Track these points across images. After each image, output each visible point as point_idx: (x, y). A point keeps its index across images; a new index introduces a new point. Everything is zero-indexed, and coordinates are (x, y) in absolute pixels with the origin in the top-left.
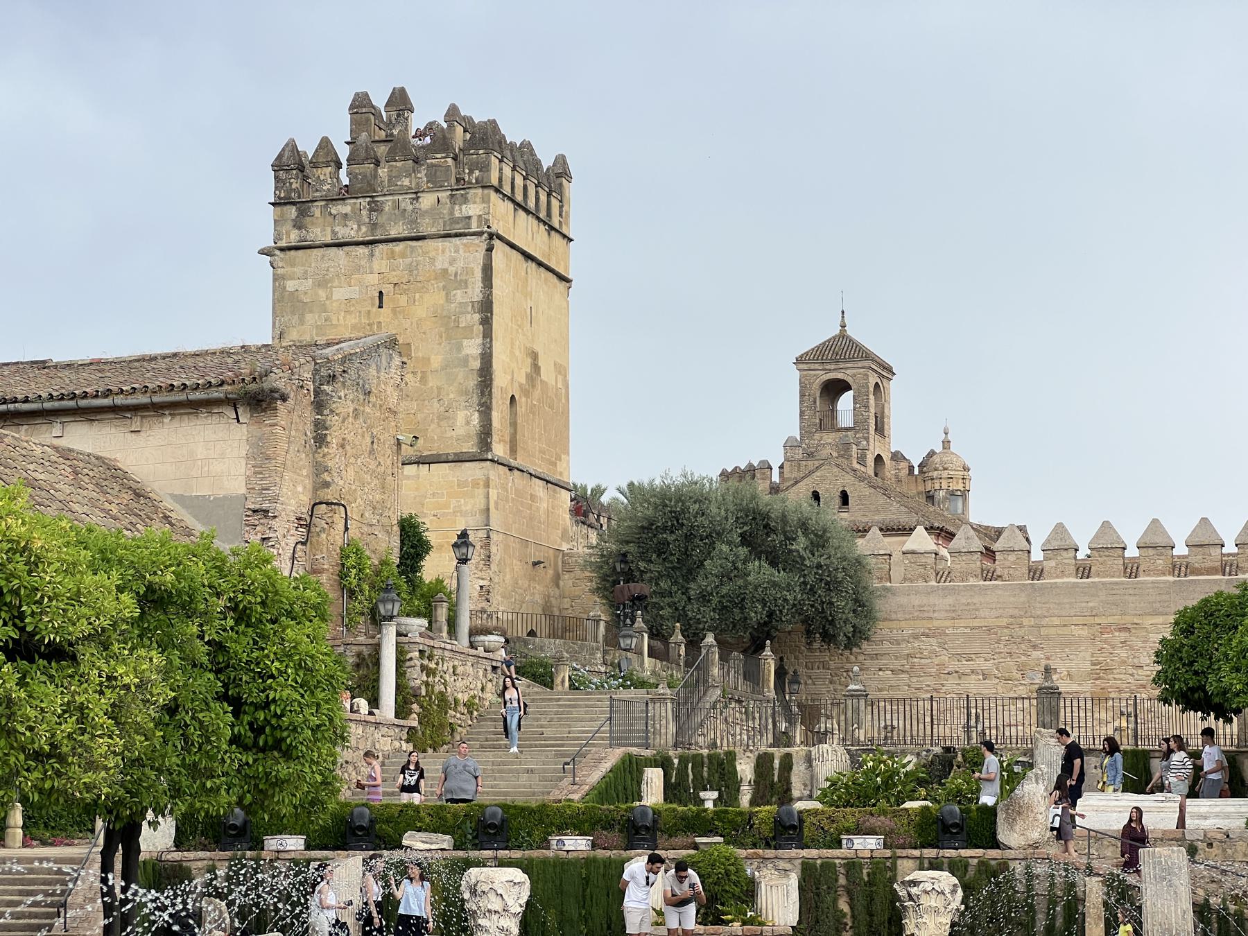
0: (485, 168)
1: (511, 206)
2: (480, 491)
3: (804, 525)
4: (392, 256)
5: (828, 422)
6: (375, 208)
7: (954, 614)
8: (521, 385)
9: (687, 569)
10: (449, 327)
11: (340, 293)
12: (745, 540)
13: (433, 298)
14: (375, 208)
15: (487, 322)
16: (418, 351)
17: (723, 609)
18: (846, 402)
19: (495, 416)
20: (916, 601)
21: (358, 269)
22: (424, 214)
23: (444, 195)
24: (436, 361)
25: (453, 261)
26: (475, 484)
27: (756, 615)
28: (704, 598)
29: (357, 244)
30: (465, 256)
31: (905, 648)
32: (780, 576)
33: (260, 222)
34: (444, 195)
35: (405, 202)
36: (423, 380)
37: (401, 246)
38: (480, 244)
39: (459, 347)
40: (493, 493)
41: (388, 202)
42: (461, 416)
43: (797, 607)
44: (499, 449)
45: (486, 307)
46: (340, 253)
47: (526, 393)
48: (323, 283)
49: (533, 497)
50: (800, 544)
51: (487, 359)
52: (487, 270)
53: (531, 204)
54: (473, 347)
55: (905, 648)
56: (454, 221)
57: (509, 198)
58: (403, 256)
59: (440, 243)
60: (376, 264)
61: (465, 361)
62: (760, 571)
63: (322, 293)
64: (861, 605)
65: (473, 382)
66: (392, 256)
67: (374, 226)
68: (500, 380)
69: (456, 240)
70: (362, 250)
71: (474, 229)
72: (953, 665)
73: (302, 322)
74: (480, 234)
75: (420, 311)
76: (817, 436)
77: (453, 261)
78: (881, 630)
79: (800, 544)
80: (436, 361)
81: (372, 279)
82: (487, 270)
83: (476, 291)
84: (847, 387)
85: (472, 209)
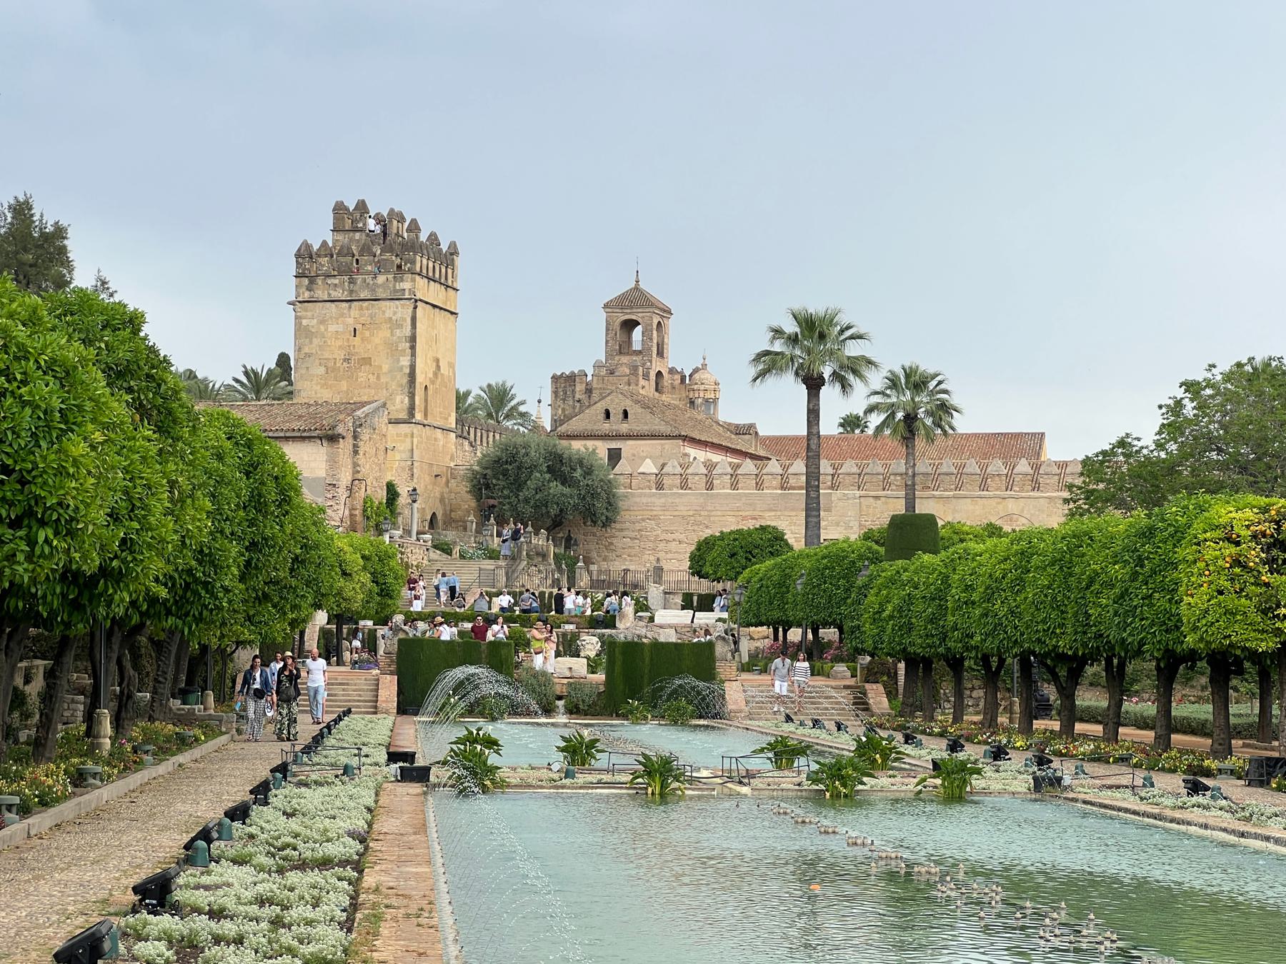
0: (413, 262)
2: (408, 440)
3: (581, 462)
4: (361, 309)
5: (624, 348)
6: (352, 281)
7: (664, 508)
9: (518, 485)
10: (393, 349)
11: (332, 328)
12: (550, 470)
13: (384, 333)
15: (413, 348)
16: (375, 362)
17: (536, 507)
18: (637, 333)
19: (417, 398)
20: (644, 500)
21: (342, 315)
22: (378, 286)
23: (390, 277)
24: (385, 368)
26: (406, 436)
27: (554, 510)
28: (527, 501)
30: (401, 311)
31: (638, 526)
32: (567, 490)
33: (288, 287)
34: (390, 277)
35: (369, 279)
36: (378, 378)
39: (398, 361)
40: (415, 440)
41: (359, 278)
42: (398, 398)
43: (575, 507)
44: (419, 416)
45: (413, 339)
46: (333, 305)
47: (433, 382)
48: (322, 322)
49: (436, 439)
50: (578, 474)
51: (413, 368)
52: (414, 319)
54: (405, 361)
55: (638, 526)
60: (352, 313)
61: (401, 369)
62: (556, 488)
63: (322, 328)
64: (611, 505)
65: (405, 380)
66: (361, 309)
67: (351, 292)
70: (344, 304)
72: (664, 536)
73: (311, 342)
75: (377, 340)
76: (617, 358)
78: (624, 516)
79: (578, 474)
80: (385, 368)
82: (414, 319)
83: (407, 331)
84: (637, 323)
85: (406, 285)
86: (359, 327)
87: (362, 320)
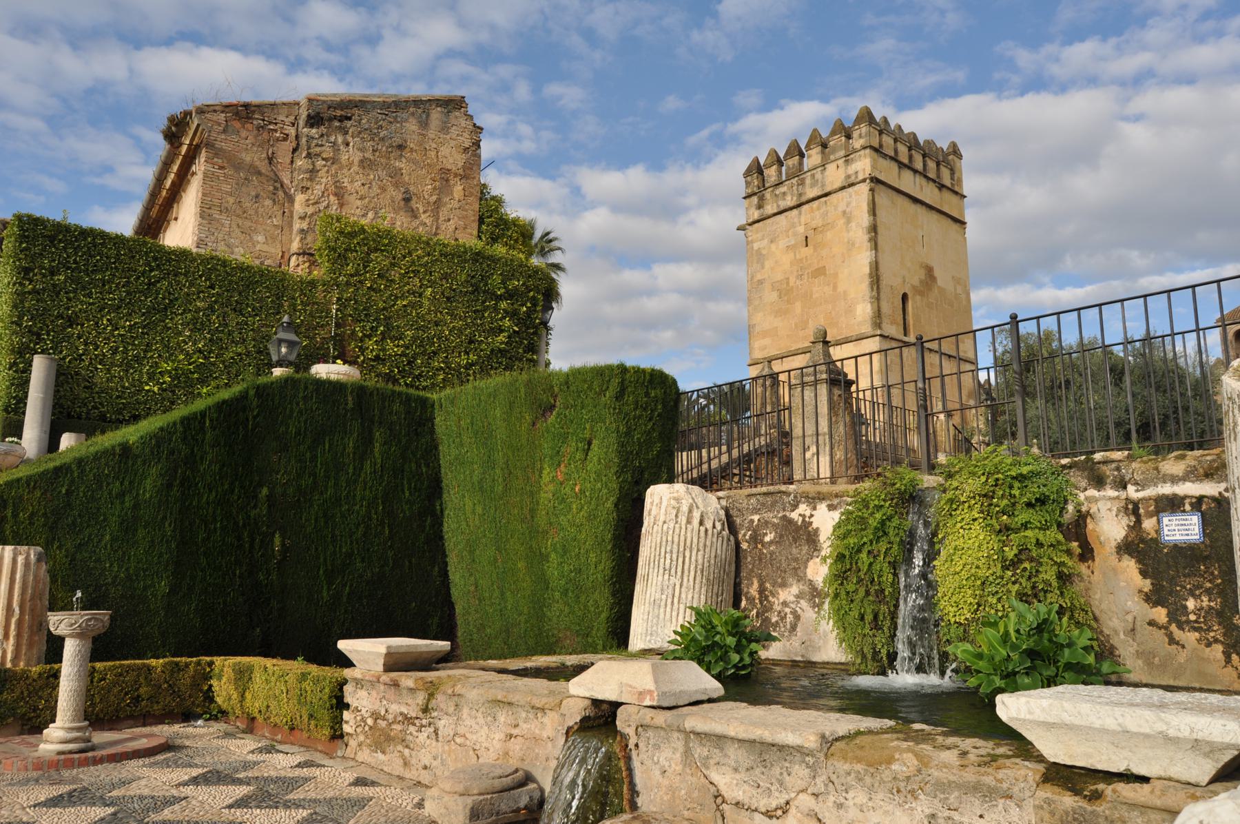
1: (894, 166)
8: (914, 287)
14: (802, 183)
25: (848, 204)
29: (791, 209)
37: (815, 204)
38: (864, 188)
53: (919, 165)
56: (849, 177)
57: (892, 158)
58: (819, 208)
59: (840, 194)
60: (803, 219)
67: (800, 195)
68: (893, 280)
69: (850, 189)
70: (795, 212)
71: (861, 177)
74: (864, 181)
77: (848, 204)
81: (801, 229)
86: (810, 234)
87: (814, 224)
